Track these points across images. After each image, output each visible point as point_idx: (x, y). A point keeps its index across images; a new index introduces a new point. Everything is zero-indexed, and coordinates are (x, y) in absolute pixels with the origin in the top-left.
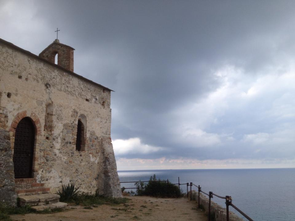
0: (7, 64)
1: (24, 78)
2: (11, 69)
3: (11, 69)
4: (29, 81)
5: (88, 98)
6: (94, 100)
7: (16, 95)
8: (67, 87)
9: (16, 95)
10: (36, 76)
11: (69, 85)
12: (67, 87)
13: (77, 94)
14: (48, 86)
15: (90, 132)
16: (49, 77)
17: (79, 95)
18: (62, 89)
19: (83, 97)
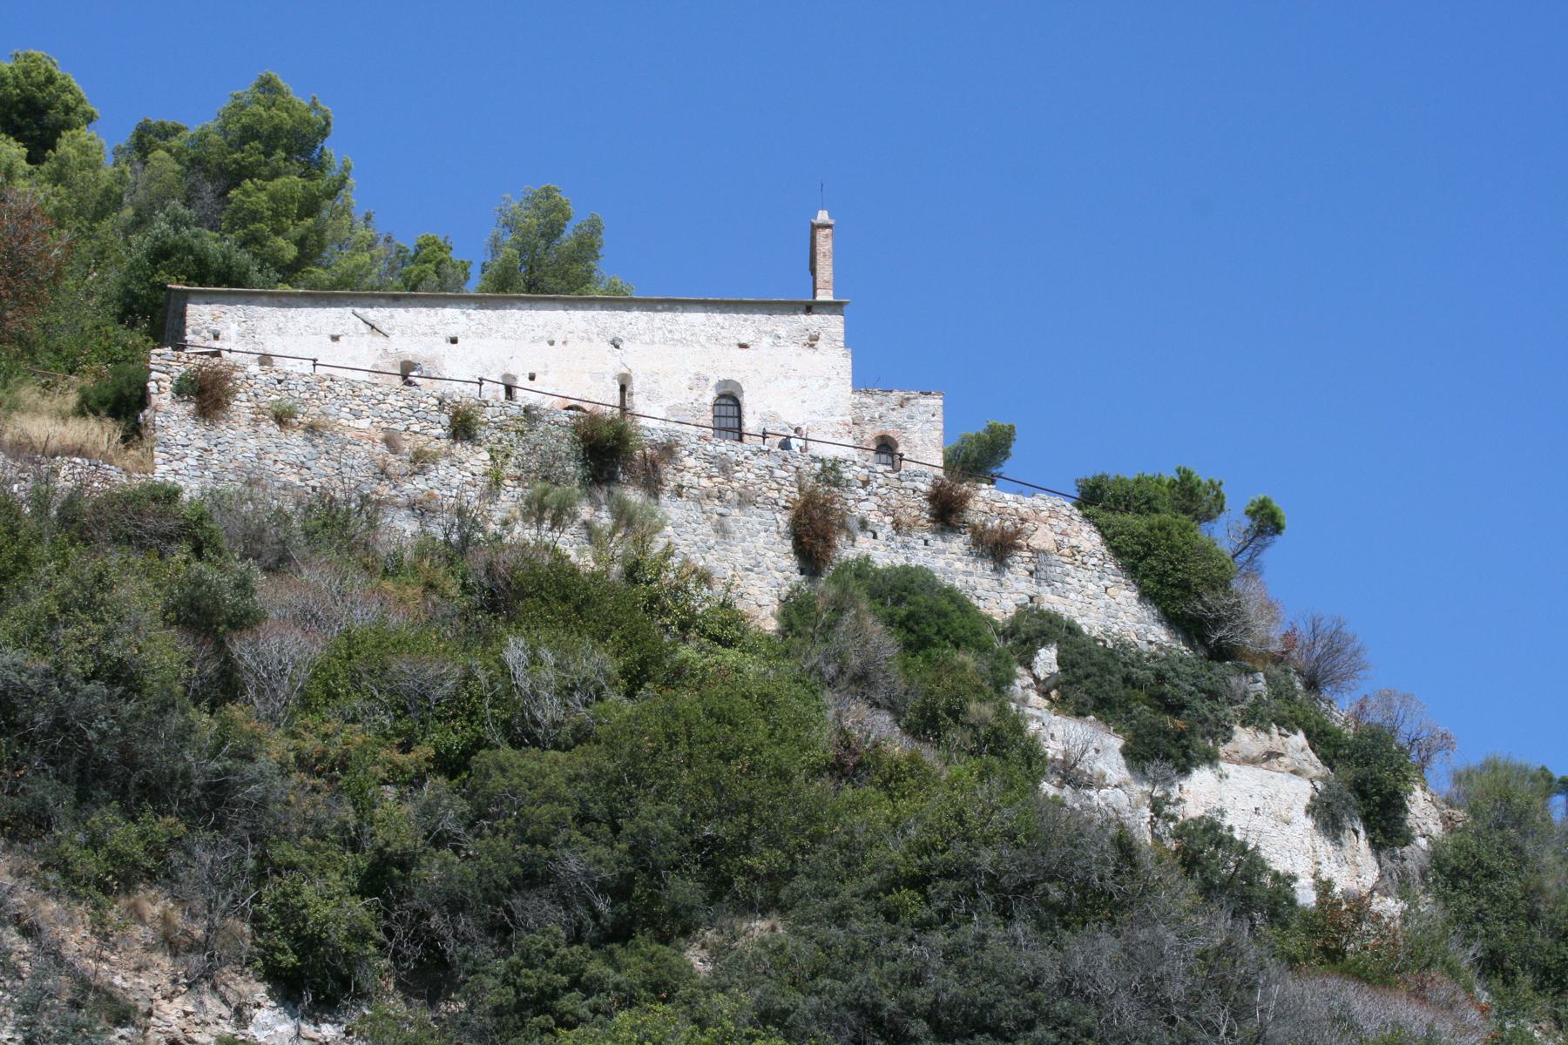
0: (523, 328)
1: (558, 343)
2: (532, 334)
3: (532, 334)
4: (569, 345)
5: (743, 341)
6: (767, 340)
7: (546, 373)
8: (670, 331)
9: (546, 373)
10: (586, 331)
11: (673, 328)
12: (670, 331)
13: (703, 339)
14: (617, 342)
15: (758, 415)
16: (617, 325)
17: (709, 339)
18: (656, 340)
19: (724, 341)
